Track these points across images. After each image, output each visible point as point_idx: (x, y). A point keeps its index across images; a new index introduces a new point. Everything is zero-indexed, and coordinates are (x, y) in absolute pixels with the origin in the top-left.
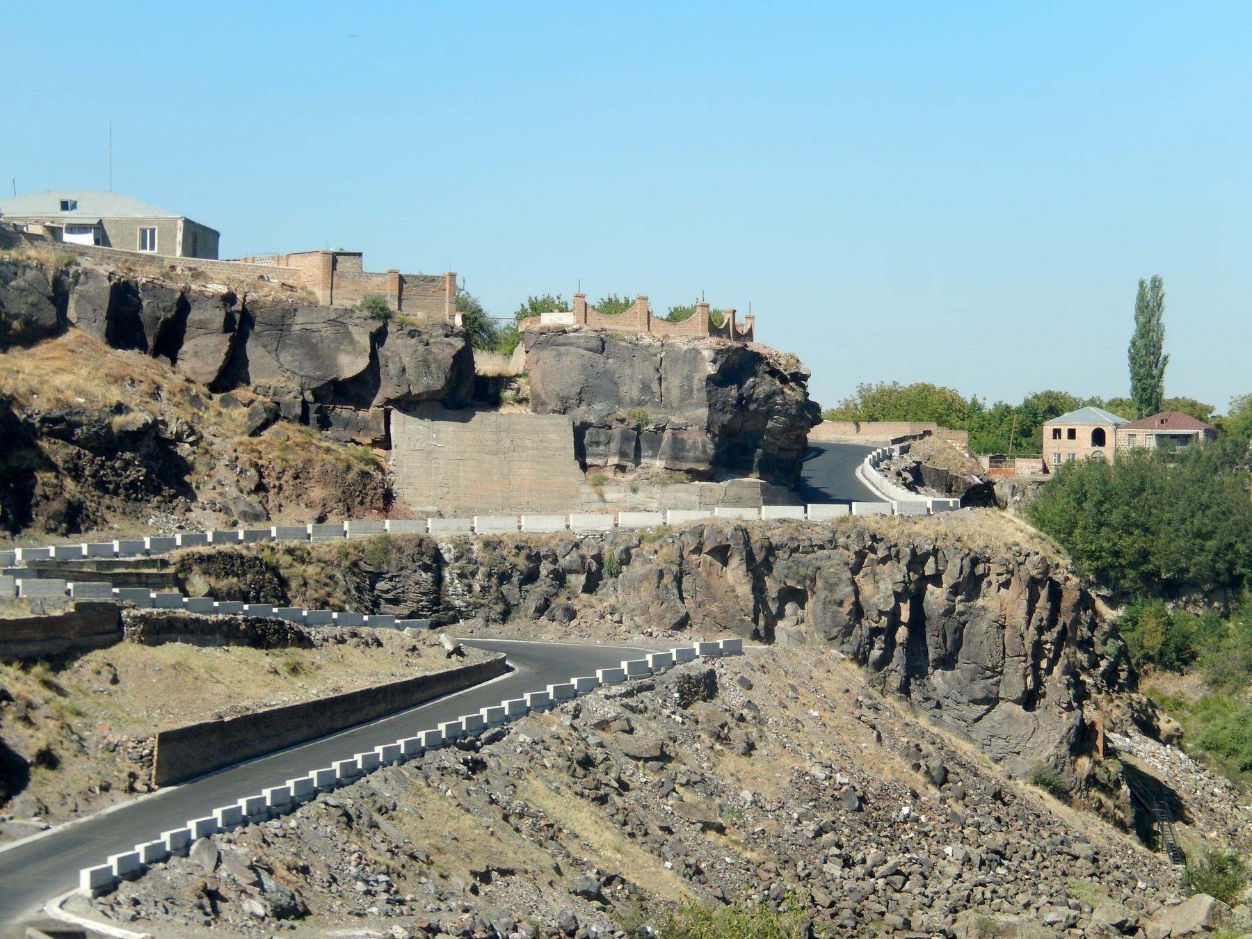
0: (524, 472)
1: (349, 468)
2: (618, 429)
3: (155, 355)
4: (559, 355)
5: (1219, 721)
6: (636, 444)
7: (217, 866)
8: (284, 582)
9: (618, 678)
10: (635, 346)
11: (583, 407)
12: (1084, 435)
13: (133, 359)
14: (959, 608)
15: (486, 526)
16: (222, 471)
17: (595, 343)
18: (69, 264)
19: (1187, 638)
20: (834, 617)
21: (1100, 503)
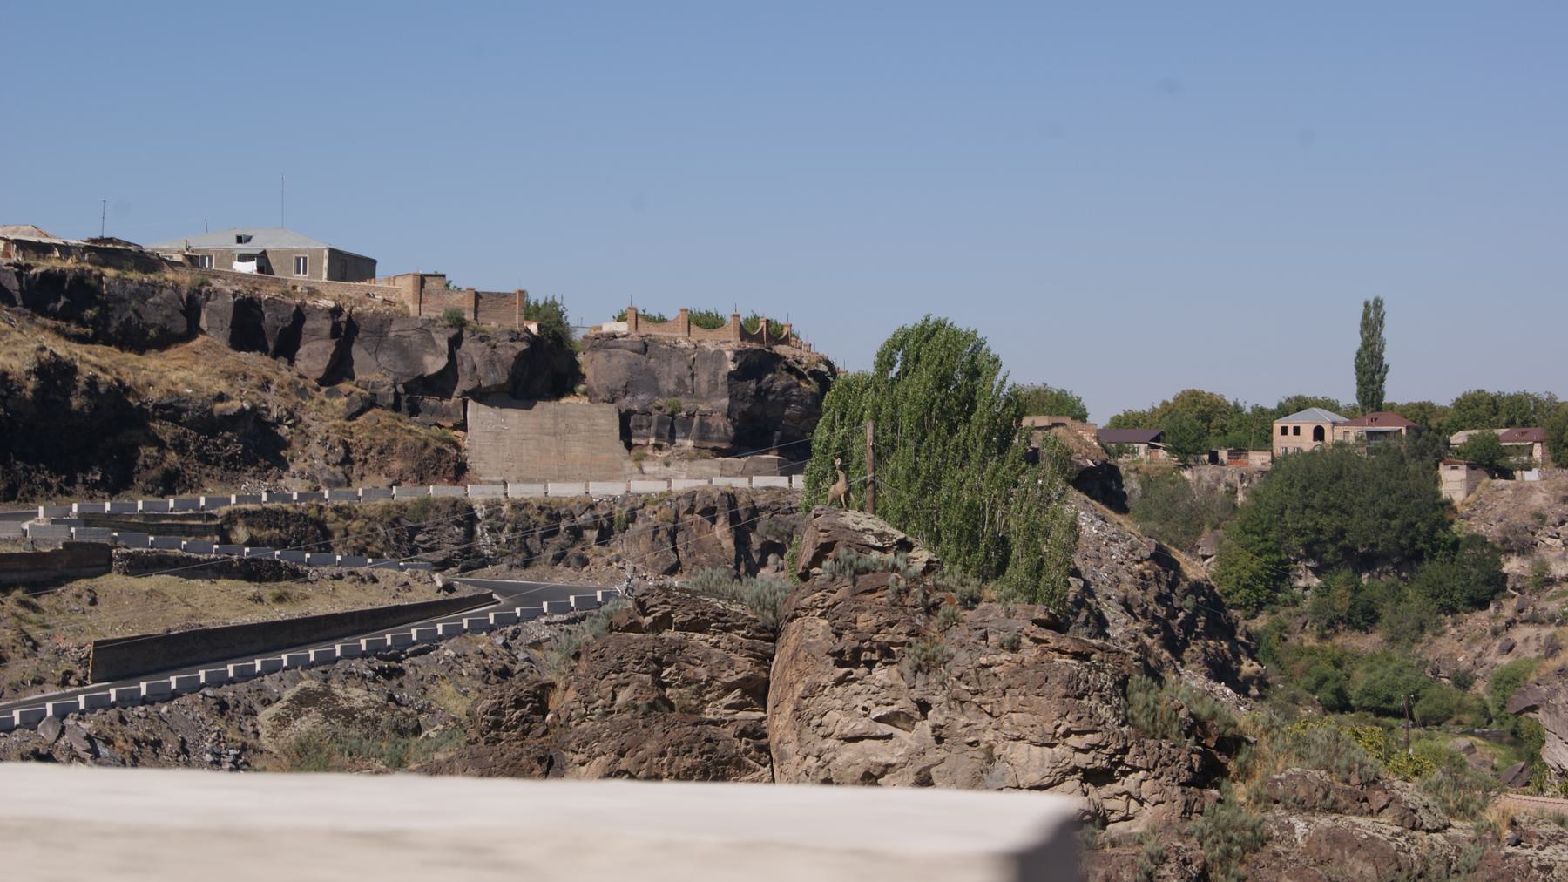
0: (577, 449)
1: (426, 445)
2: (656, 414)
3: (275, 357)
4: (610, 356)
5: (1380, 672)
6: (670, 428)
7: (59, 737)
8: (327, 534)
11: (628, 398)
12: (1307, 431)
13: (254, 360)
15: (517, 491)
16: (314, 448)
17: (639, 346)
18: (202, 285)
21: (1304, 488)
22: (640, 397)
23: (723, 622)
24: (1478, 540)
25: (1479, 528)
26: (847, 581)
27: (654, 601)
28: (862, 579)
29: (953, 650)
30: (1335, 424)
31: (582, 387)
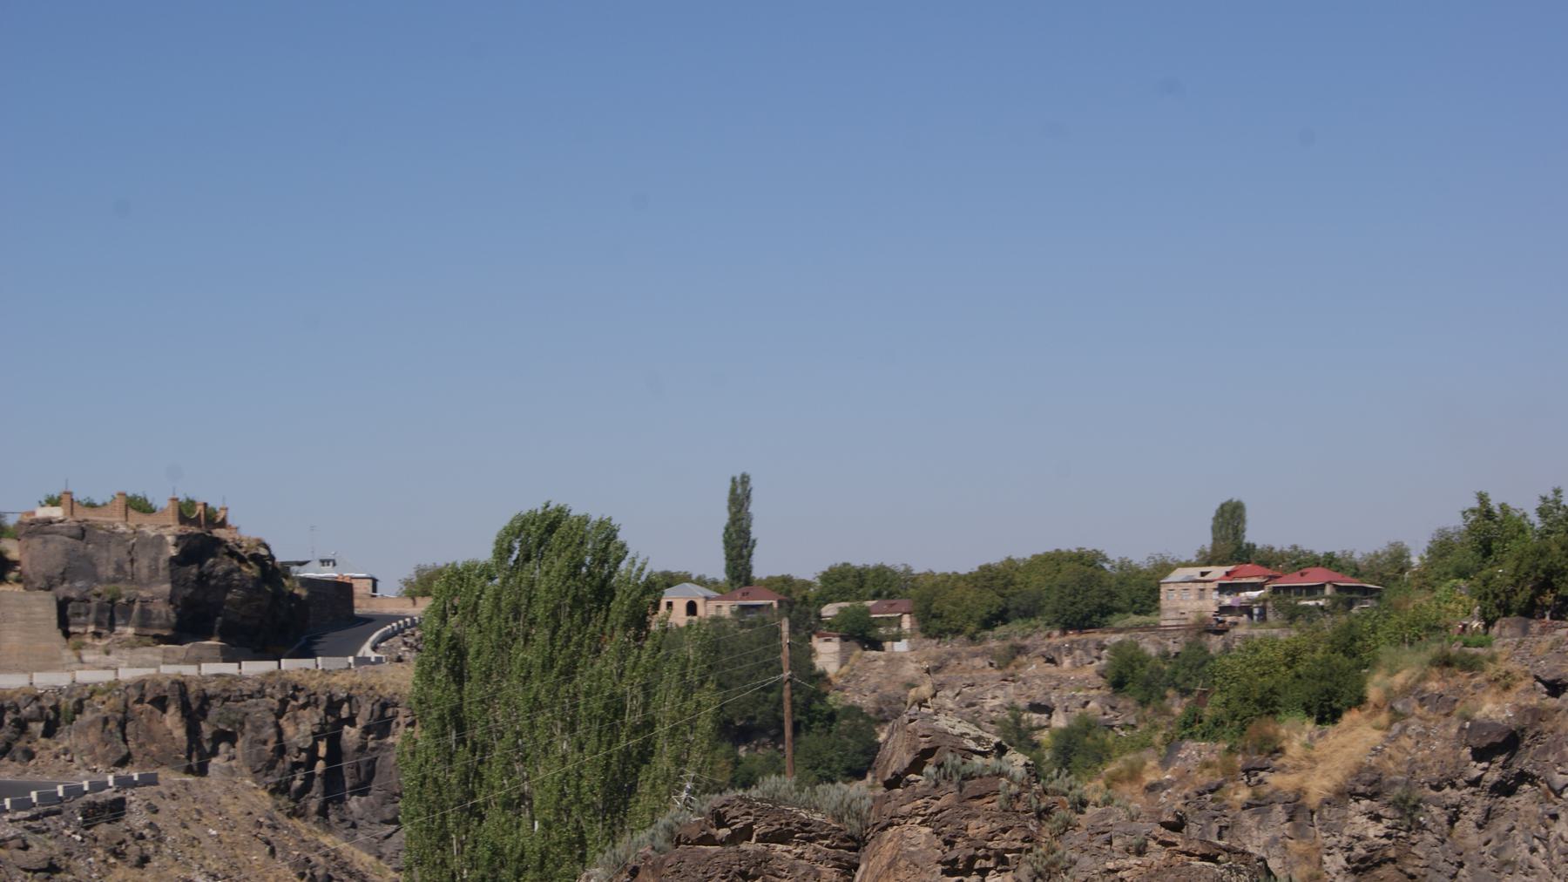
0: (14, 639)
4: (46, 542)
6: (110, 615)
9: (28, 805)
10: (112, 534)
11: (66, 585)
14: (371, 744)
17: (75, 532)
19: (751, 774)
20: (259, 753)
22: (78, 584)
23: (808, 832)
24: (854, 711)
25: (856, 699)
26: (953, 788)
27: (734, 812)
28: (968, 784)
29: (1075, 856)
30: (707, 599)
31: (13, 575)
